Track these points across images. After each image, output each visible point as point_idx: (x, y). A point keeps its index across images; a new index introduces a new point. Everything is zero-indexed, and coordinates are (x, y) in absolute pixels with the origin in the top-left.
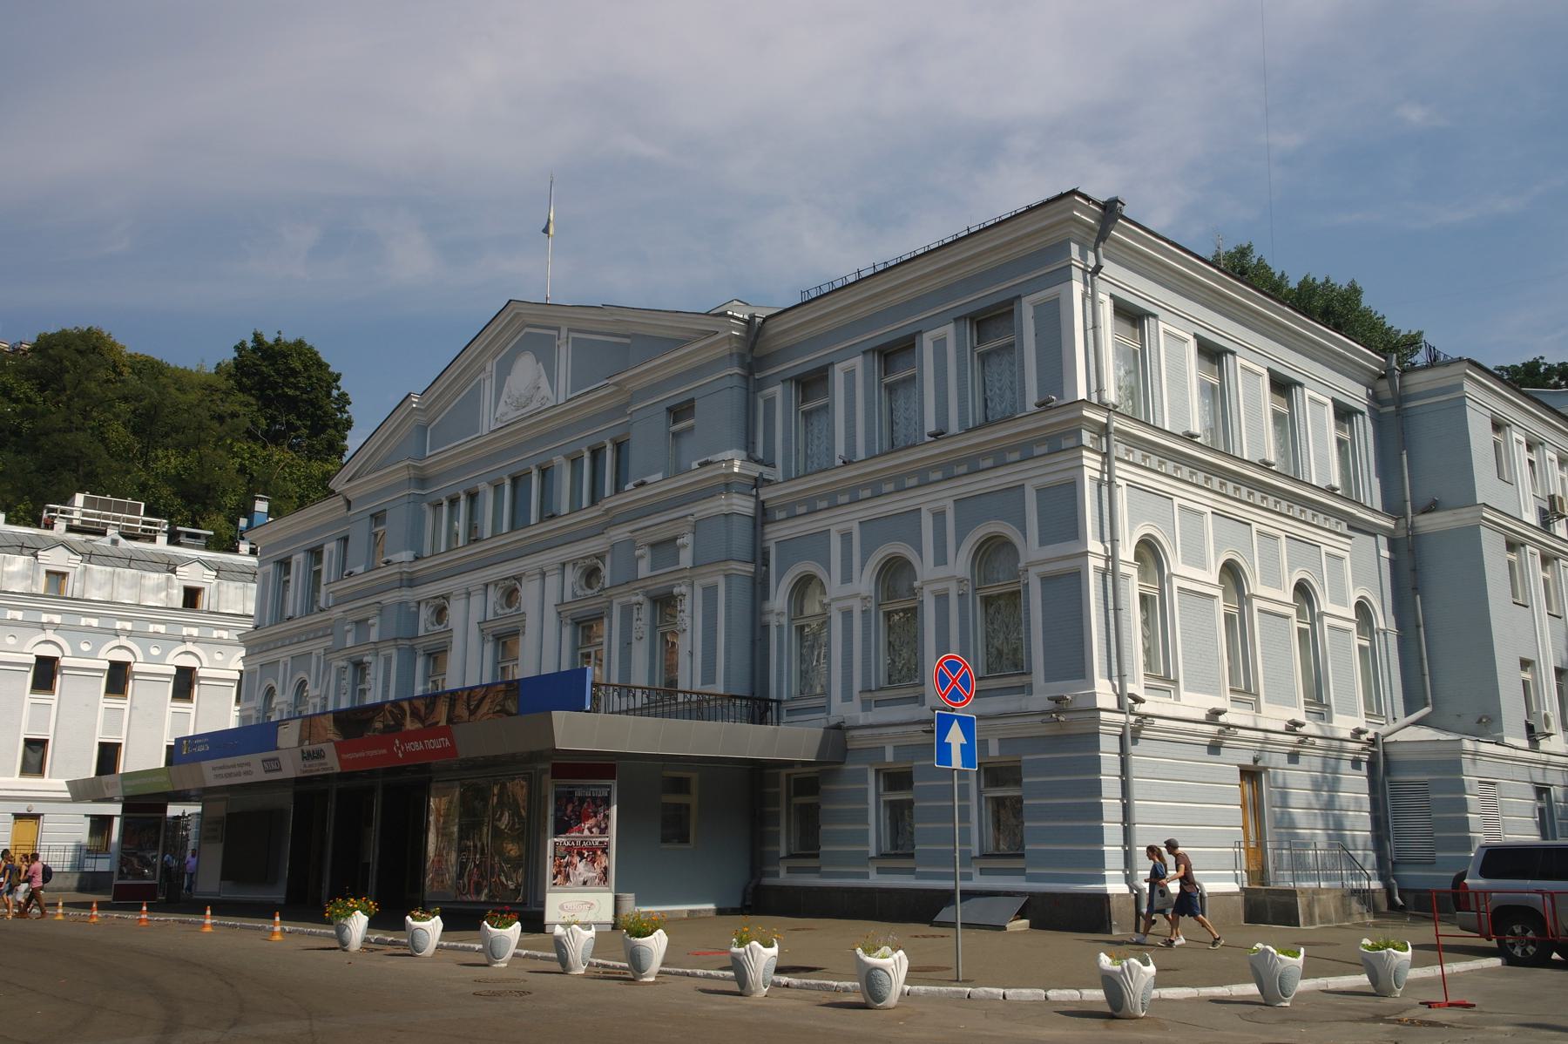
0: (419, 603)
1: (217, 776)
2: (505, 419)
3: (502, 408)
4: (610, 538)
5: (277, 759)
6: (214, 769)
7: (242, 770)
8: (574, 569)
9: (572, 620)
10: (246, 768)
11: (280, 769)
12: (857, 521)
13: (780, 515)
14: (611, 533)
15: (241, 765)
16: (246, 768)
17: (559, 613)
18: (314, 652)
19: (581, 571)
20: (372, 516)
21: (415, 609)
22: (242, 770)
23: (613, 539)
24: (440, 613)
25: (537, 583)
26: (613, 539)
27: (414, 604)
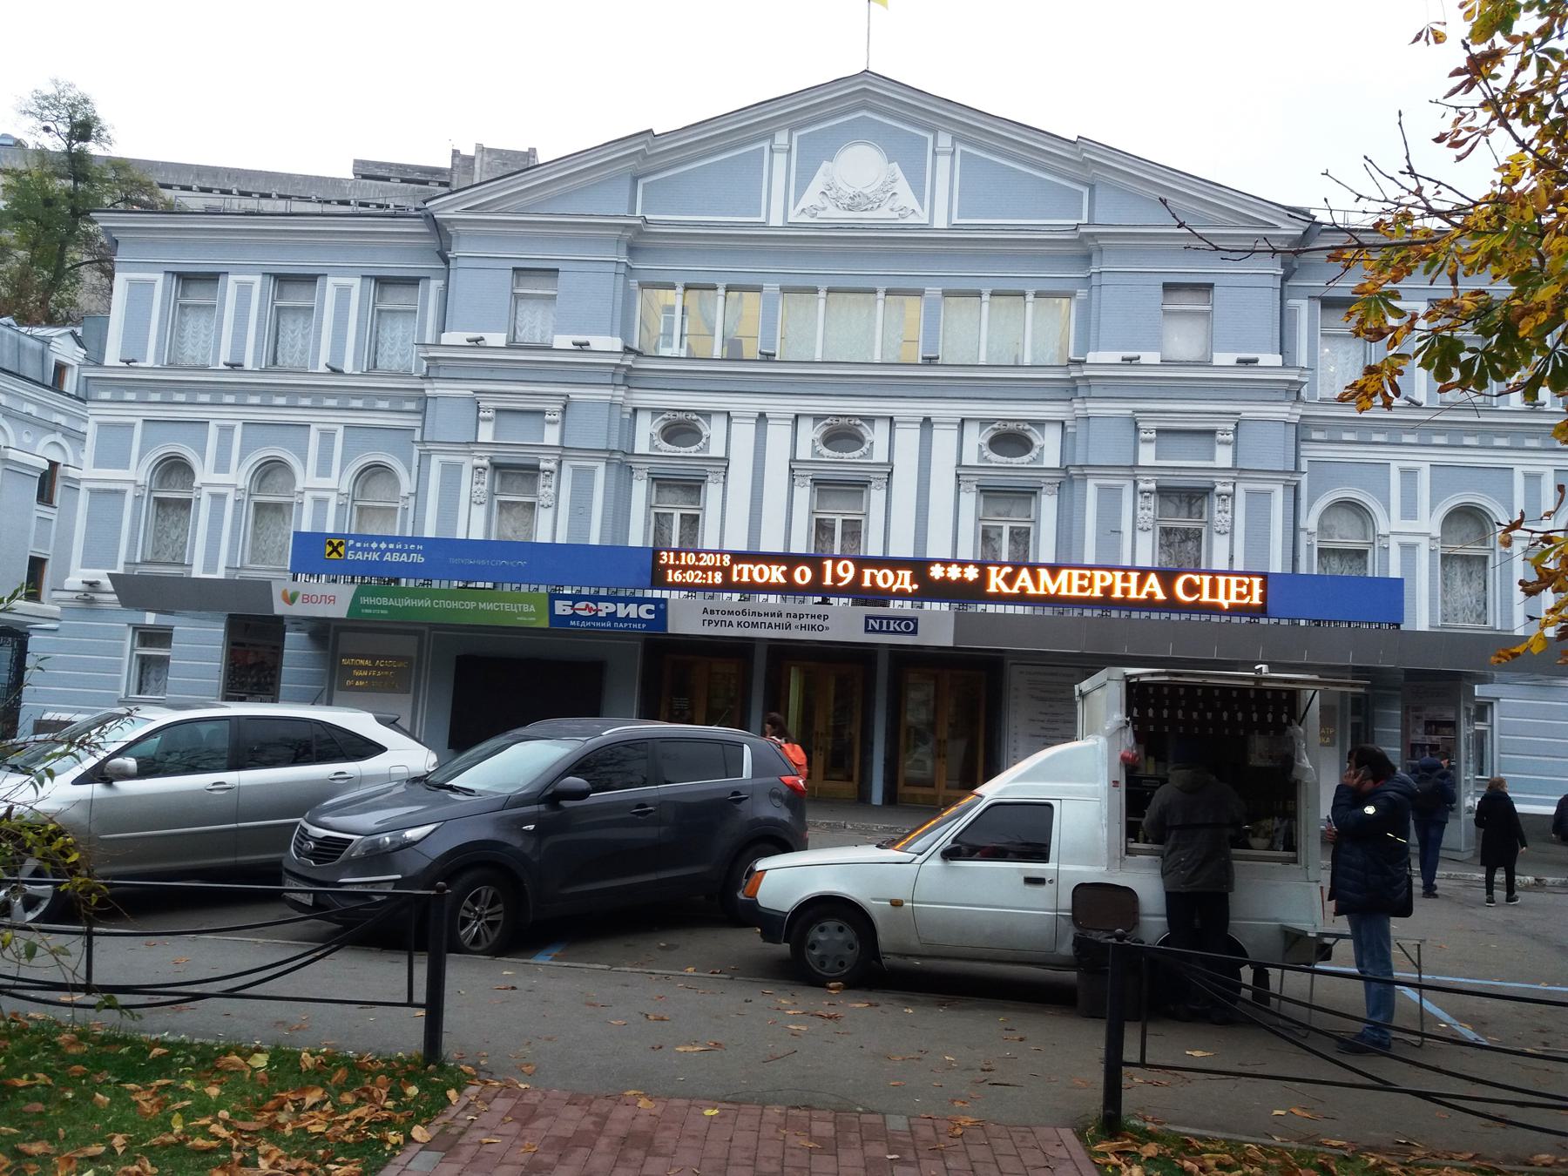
0: (635, 410)
2: (820, 214)
3: (811, 197)
4: (1086, 409)
7: (795, 622)
8: (980, 432)
9: (977, 486)
11: (915, 632)
12: (1429, 463)
13: (1316, 435)
14: (1088, 405)
17: (958, 476)
18: (313, 427)
19: (992, 433)
20: (515, 269)
21: (628, 416)
23: (1089, 411)
24: (680, 430)
25: (953, 435)
26: (1089, 411)
27: (630, 410)
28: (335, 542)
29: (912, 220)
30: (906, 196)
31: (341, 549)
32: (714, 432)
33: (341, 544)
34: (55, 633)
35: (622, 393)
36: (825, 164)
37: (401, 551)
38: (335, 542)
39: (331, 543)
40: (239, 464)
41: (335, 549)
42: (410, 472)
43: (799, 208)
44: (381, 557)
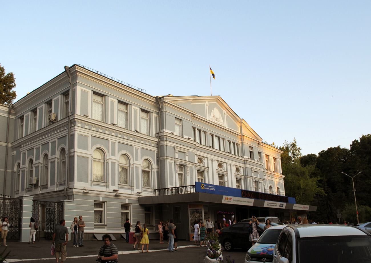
1: (268, 205)
3: (211, 117)
5: (283, 204)
6: (268, 203)
7: (275, 205)
10: (276, 205)
15: (275, 204)
16: (276, 205)
22: (275, 205)
28: (203, 185)
29: (223, 125)
30: (222, 121)
31: (203, 187)
32: (205, 161)
33: (203, 185)
34: (73, 203)
35: (195, 151)
36: (213, 111)
37: (212, 188)
38: (203, 185)
39: (202, 185)
40: (91, 149)
41: (203, 187)
42: (154, 162)
43: (211, 118)
44: (209, 189)
